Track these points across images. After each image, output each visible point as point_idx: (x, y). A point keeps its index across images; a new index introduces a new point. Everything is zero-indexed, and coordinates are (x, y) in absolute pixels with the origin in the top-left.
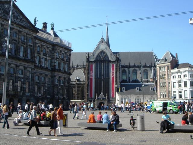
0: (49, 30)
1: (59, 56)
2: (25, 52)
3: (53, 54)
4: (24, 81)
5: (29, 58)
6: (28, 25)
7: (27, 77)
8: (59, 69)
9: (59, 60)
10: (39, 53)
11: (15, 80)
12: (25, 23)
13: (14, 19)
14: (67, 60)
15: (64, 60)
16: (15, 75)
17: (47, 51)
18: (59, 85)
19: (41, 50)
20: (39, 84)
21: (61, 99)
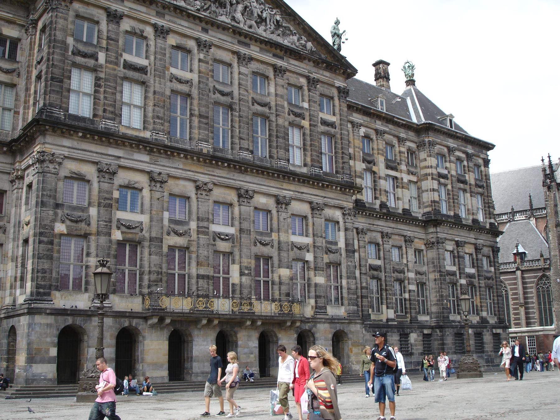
0: (397, 86)
1: (446, 168)
2: (310, 145)
3: (425, 160)
4: (315, 257)
5: (328, 171)
6: (309, 45)
7: (329, 242)
8: (452, 213)
9: (449, 182)
10: (369, 159)
11: (279, 255)
12: (295, 38)
13: (249, 22)
14: (476, 180)
15: (464, 182)
16: (274, 236)
17: (400, 152)
18: (460, 273)
19: (378, 149)
20: (382, 275)
21: (472, 327)
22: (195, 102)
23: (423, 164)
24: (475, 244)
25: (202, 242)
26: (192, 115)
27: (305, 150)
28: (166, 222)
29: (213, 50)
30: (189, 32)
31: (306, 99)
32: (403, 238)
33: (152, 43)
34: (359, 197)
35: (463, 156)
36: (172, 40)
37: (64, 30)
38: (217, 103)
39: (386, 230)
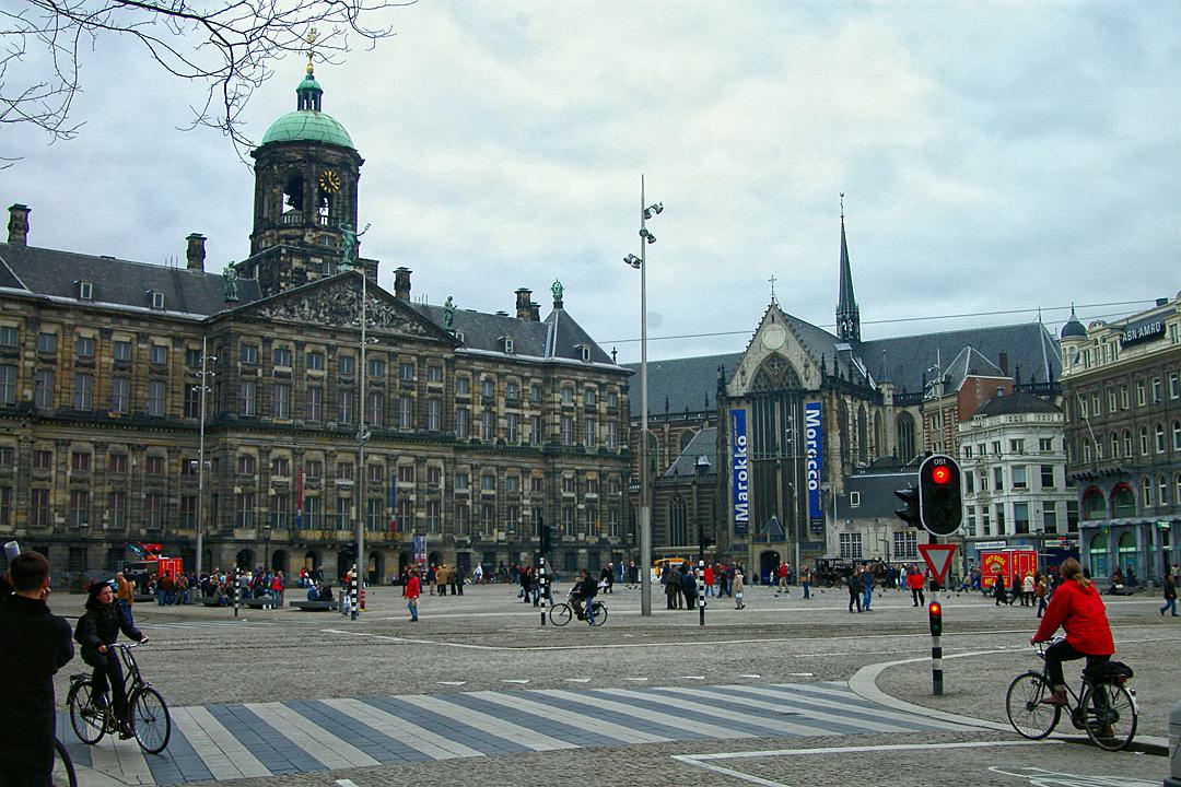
3: (549, 395)
15: (595, 412)
16: (384, 484)
19: (499, 391)
22: (325, 392)
23: (549, 399)
24: (599, 471)
25: (329, 492)
26: (323, 402)
27: (413, 415)
28: (304, 481)
29: (339, 349)
30: (320, 341)
31: (416, 373)
32: (520, 470)
33: (294, 355)
34: (475, 437)
35: (595, 386)
36: (308, 349)
37: (235, 359)
38: (342, 390)
39: (501, 463)
